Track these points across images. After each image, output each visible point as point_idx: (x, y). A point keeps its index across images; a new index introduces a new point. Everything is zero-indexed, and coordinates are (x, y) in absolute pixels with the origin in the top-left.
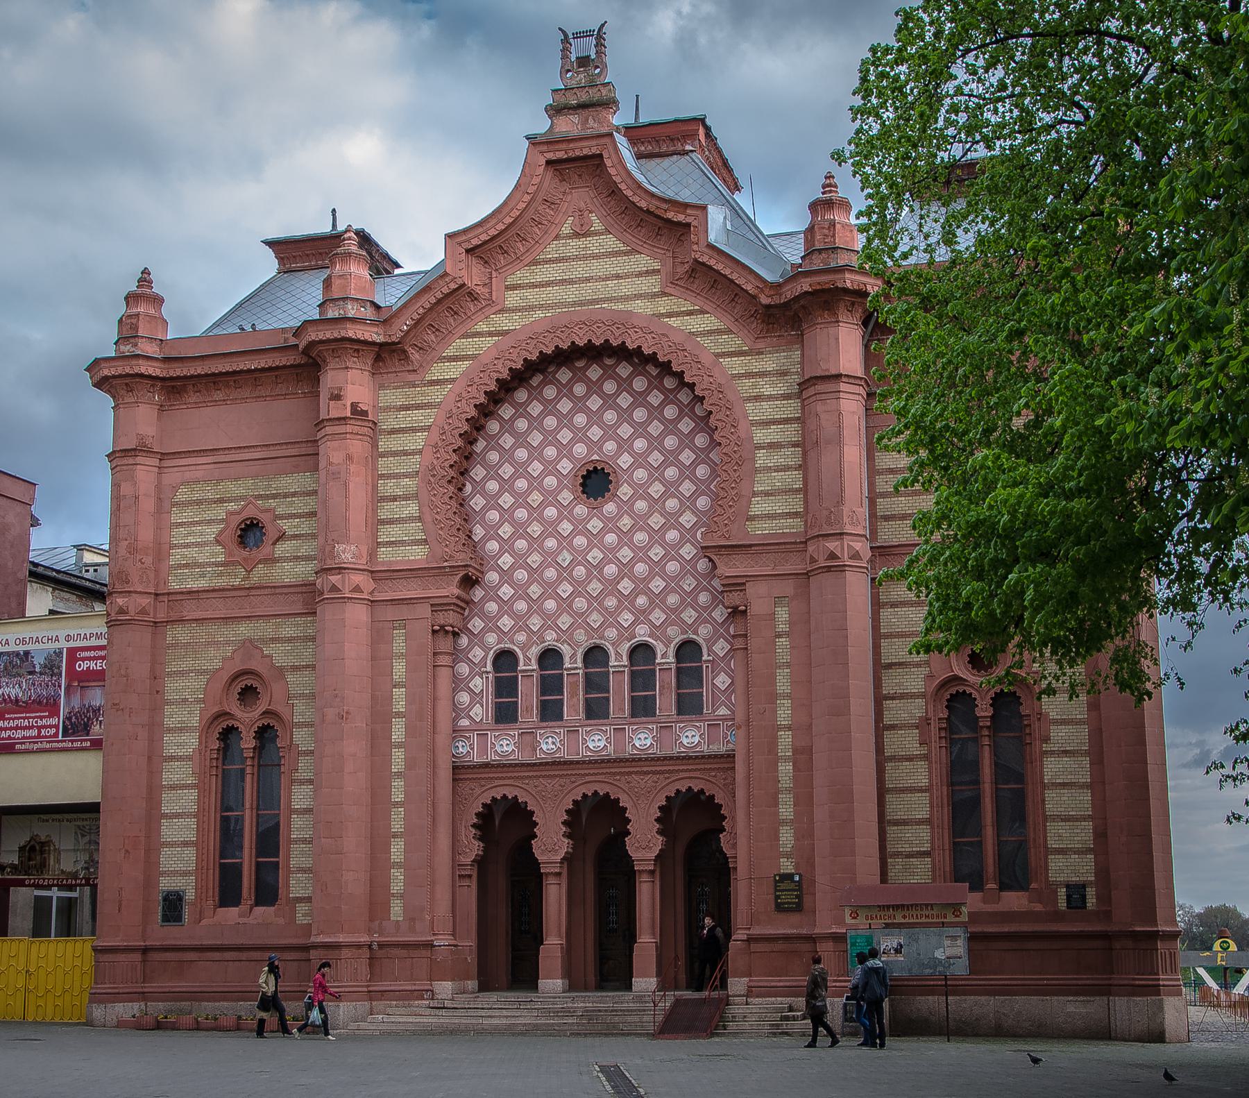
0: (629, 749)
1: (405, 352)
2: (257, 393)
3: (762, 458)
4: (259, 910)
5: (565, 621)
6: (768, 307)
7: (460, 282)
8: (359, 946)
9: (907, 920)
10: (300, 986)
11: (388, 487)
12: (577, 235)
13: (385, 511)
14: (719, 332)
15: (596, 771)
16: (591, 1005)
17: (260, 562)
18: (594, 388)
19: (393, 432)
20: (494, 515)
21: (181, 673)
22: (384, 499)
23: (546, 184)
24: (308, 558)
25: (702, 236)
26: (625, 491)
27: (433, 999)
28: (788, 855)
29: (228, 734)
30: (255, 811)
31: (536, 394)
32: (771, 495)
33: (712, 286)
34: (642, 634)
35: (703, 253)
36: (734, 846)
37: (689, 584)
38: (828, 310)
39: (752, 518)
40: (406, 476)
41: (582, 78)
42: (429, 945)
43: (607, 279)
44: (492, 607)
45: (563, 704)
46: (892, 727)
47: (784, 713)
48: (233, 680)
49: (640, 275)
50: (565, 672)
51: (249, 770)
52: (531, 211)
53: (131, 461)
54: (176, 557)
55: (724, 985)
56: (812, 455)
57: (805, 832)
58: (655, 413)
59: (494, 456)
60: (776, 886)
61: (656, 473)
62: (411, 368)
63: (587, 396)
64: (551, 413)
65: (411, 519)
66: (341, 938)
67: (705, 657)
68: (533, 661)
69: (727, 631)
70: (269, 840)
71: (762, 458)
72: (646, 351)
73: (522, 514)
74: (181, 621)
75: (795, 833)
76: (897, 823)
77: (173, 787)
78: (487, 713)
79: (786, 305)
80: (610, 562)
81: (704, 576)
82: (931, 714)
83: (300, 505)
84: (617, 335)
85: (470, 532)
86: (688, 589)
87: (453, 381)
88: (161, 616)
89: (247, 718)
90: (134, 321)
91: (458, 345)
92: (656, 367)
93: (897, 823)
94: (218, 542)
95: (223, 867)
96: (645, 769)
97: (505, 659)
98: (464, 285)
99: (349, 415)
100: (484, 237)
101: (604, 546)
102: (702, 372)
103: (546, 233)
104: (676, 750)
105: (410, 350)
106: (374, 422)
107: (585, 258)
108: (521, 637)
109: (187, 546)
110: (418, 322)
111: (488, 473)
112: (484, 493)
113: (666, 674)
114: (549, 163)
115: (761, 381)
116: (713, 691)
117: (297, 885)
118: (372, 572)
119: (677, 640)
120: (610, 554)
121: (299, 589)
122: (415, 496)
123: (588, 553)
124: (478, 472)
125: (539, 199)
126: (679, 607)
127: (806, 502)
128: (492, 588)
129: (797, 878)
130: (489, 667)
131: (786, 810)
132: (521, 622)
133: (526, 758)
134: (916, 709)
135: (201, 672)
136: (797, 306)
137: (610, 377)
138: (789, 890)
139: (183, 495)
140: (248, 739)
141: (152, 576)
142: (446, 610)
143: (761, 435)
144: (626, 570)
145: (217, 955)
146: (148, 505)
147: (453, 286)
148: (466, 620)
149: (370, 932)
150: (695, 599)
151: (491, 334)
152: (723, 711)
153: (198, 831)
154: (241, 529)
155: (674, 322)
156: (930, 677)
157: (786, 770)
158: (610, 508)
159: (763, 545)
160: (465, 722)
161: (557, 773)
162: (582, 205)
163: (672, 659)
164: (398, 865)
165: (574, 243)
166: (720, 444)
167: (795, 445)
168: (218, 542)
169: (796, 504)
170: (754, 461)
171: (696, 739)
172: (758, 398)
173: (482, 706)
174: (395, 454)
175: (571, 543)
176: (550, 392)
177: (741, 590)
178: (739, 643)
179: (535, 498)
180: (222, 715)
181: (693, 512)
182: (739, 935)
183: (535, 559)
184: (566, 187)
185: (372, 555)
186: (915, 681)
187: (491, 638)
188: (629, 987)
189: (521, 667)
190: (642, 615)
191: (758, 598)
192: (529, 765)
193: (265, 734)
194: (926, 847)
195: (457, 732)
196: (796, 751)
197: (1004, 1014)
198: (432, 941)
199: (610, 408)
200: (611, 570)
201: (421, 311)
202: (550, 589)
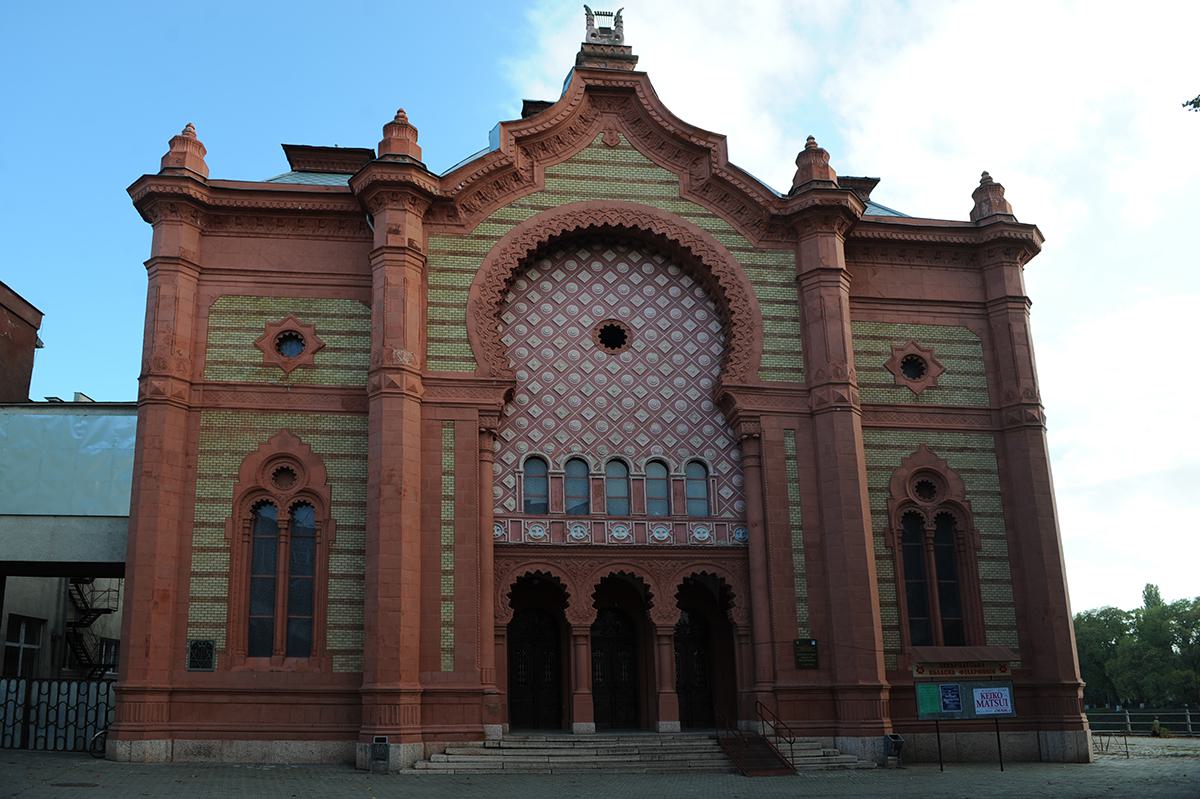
0: (649, 541)
2: (299, 232)
3: (768, 327)
4: (291, 660)
6: (774, 217)
7: (510, 160)
13: (435, 331)
14: (729, 232)
17: (299, 366)
18: (609, 266)
24: (348, 368)
25: (721, 158)
26: (638, 345)
28: (803, 625)
31: (559, 264)
34: (657, 451)
35: (722, 171)
37: (695, 418)
39: (761, 369)
44: (524, 421)
47: (795, 517)
49: (661, 183)
50: (591, 477)
51: (283, 539)
52: (571, 121)
53: (172, 267)
54: (213, 354)
58: (662, 290)
61: (664, 333)
64: (572, 281)
68: (562, 466)
69: (728, 455)
70: (305, 599)
74: (217, 408)
77: (203, 550)
78: (520, 504)
83: (339, 325)
86: (693, 420)
88: (196, 402)
90: (181, 157)
91: (503, 212)
92: (663, 257)
98: (511, 164)
100: (533, 131)
107: (614, 164)
108: (551, 447)
110: (471, 186)
111: (517, 319)
112: (514, 333)
114: (588, 88)
117: (335, 640)
121: (339, 392)
124: (509, 317)
126: (687, 435)
127: (807, 361)
128: (522, 407)
129: (814, 643)
130: (521, 469)
131: (801, 590)
133: (557, 542)
135: (235, 453)
137: (623, 261)
141: (188, 367)
143: (766, 310)
144: (642, 404)
146: (187, 307)
147: (504, 162)
150: (700, 430)
151: (533, 207)
155: (693, 220)
157: (799, 559)
158: (626, 355)
159: (775, 389)
160: (499, 511)
162: (611, 126)
163: (683, 473)
165: (606, 151)
167: (795, 320)
168: (256, 346)
172: (763, 283)
176: (572, 265)
177: (756, 422)
183: (561, 388)
184: (597, 111)
187: (523, 446)
190: (656, 438)
191: (770, 428)
196: (807, 545)
200: (628, 402)
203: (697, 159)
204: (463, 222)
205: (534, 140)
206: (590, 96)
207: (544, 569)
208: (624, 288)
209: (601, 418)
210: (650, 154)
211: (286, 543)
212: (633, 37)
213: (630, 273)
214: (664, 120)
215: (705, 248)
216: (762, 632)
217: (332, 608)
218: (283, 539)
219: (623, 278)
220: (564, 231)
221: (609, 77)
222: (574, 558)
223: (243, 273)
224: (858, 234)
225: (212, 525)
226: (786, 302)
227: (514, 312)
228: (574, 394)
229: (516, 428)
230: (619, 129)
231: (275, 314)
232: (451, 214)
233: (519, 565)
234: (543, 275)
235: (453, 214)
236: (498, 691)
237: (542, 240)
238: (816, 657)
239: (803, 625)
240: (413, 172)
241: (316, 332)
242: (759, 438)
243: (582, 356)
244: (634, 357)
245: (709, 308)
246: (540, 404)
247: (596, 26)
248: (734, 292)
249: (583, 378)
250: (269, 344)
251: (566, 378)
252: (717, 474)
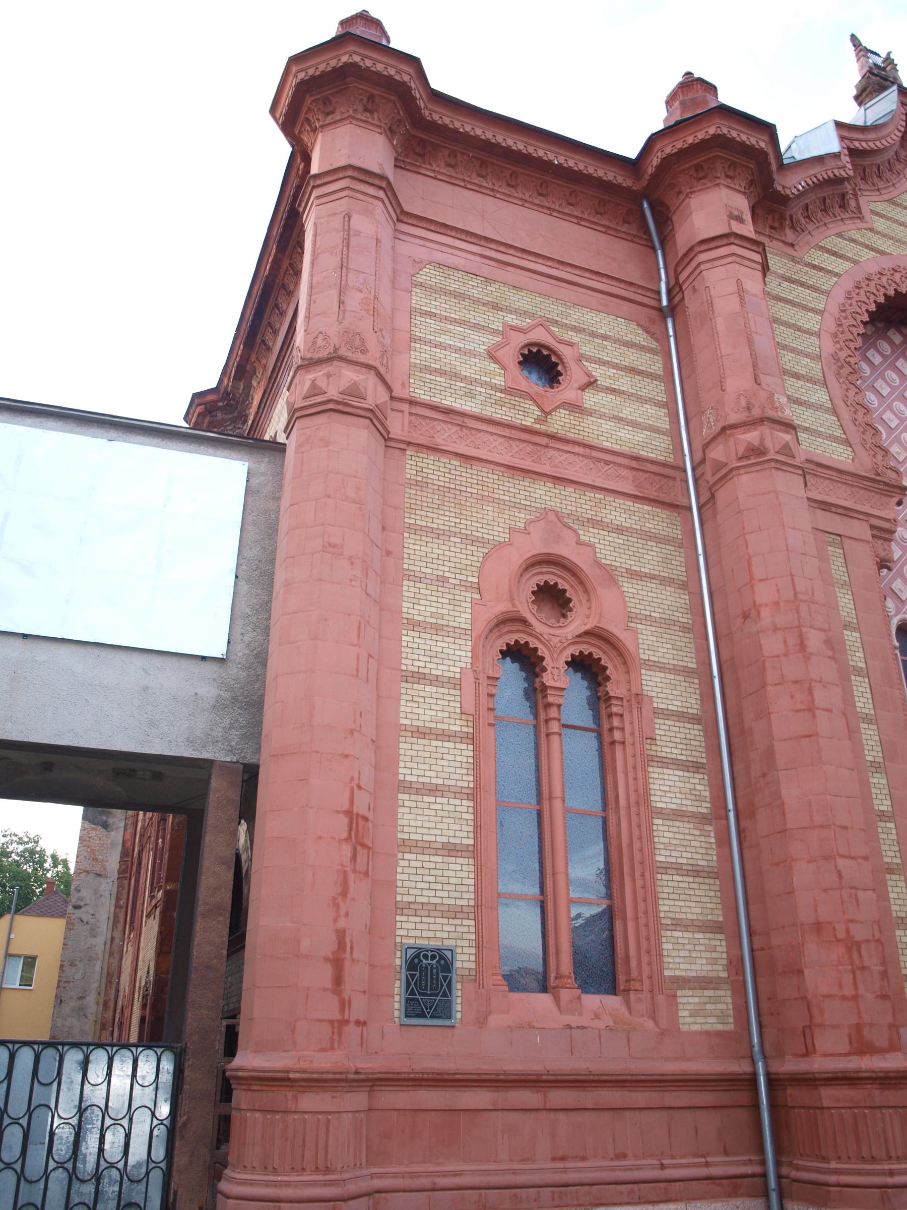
1: (782, 218)
10: (707, 1165)
21: (437, 534)
24: (634, 424)
48: (526, 569)
121: (626, 462)
180: (515, 620)
225: (435, 681)
231: (515, 311)
232: (776, 225)
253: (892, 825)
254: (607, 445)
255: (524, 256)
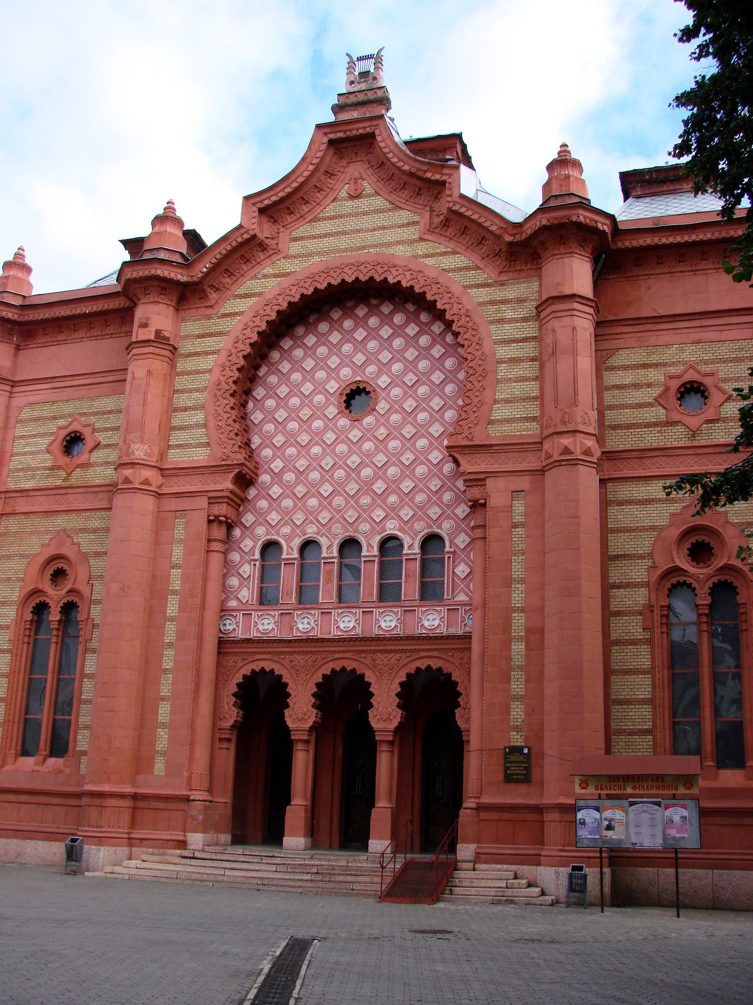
0: (376, 631)
1: (204, 291)
2: (91, 334)
3: (503, 371)
4: (52, 761)
5: (324, 516)
6: (511, 244)
7: (252, 233)
8: (122, 796)
9: (637, 791)
11: (181, 400)
12: (352, 197)
14: (467, 268)
15: (344, 649)
16: (327, 863)
18: (361, 322)
19: (190, 355)
20: (270, 427)
22: (177, 410)
23: (328, 159)
26: (382, 406)
27: (185, 849)
28: (517, 729)
29: (41, 609)
30: (56, 675)
31: (311, 328)
32: (511, 402)
33: (463, 233)
35: (455, 203)
36: (468, 720)
38: (564, 244)
39: (491, 422)
40: (197, 390)
41: (363, 86)
42: (187, 800)
43: (374, 230)
45: (319, 590)
46: (618, 614)
47: (518, 596)
50: (323, 561)
52: (315, 179)
55: (453, 850)
56: (549, 366)
57: (535, 708)
59: (273, 379)
60: (505, 758)
62: (208, 304)
63: (354, 330)
65: (198, 426)
66: (106, 788)
67: (447, 549)
68: (295, 551)
71: (503, 371)
72: (405, 284)
73: (293, 426)
75: (525, 708)
76: (620, 702)
79: (525, 244)
80: (367, 466)
81: (448, 478)
82: (653, 601)
83: (113, 421)
84: (380, 272)
85: (249, 440)
87: (242, 313)
89: (55, 596)
91: (249, 285)
92: (413, 304)
93: (620, 702)
94: (48, 451)
95: (26, 720)
96: (389, 648)
97: (270, 547)
99: (152, 337)
100: (274, 199)
101: (362, 453)
102: (452, 301)
103: (326, 196)
104: (419, 631)
105: (209, 290)
106: (173, 346)
107: (357, 215)
108: (286, 530)
109: (25, 454)
113: (410, 564)
114: (331, 142)
115: (503, 307)
116: (453, 579)
117: (82, 741)
118: (161, 470)
119: (422, 534)
120: (367, 459)
122: (202, 407)
123: (347, 459)
124: (259, 392)
125: (322, 170)
127: (542, 407)
129: (526, 751)
130: (257, 556)
131: (518, 686)
132: (287, 516)
133: (286, 636)
134: (639, 597)
135: (23, 556)
136: (536, 243)
137: (375, 314)
138: (517, 762)
139: (26, 414)
140: (55, 613)
142: (221, 503)
143: (503, 352)
145: (12, 797)
147: (246, 236)
148: (239, 515)
149: (133, 784)
150: (440, 499)
151: (275, 276)
152: (462, 597)
153: (8, 689)
154: (67, 441)
155: (429, 261)
156: (654, 567)
157: (518, 649)
158: (369, 420)
160: (233, 604)
161: (310, 649)
162: (356, 175)
163: (417, 550)
164: (163, 725)
166: (466, 359)
167: (533, 360)
168: (48, 451)
169: (533, 410)
170: (496, 372)
171: (436, 623)
172: (501, 321)
173: (249, 589)
174: (189, 373)
175: (333, 451)
176: (323, 327)
177: (481, 485)
178: (479, 533)
179: (306, 413)
181: (441, 424)
182: (469, 803)
183: (302, 464)
184: (344, 162)
185: (162, 456)
186: (639, 572)
187: (260, 531)
188: (365, 848)
189: (284, 556)
190: (392, 512)
192: (285, 641)
193: (69, 608)
194: (648, 725)
195: (224, 612)
196: (529, 631)
197: (722, 888)
198: (189, 796)
199: (373, 338)
200: (366, 472)
201: (219, 256)
202: (313, 490)
203: (438, 193)
204: (213, 302)
205: (280, 207)
206: (336, 149)
207: (268, 666)
208: (372, 345)
209: (339, 494)
210: (393, 197)
211: (57, 643)
212: (388, 79)
213: (380, 327)
214: (400, 160)
215: (442, 290)
216: (474, 740)
217: (85, 709)
218: (54, 639)
219: (372, 334)
220: (302, 295)
221: (350, 127)
222: (299, 653)
223: (44, 382)
224: (620, 245)
226: (525, 340)
227: (265, 385)
228: (314, 469)
229: (256, 510)
230: (364, 176)
232: (203, 296)
233: (246, 661)
234: (295, 342)
235: (203, 296)
236: (210, 798)
237: (281, 308)
238: (528, 769)
239: (517, 729)
240: (157, 266)
241: (94, 431)
242: (484, 505)
243: (326, 425)
244: (377, 420)
245: (459, 354)
246: (280, 483)
247: (357, 73)
248: (467, 336)
249: (324, 450)
250: (57, 448)
251: (308, 453)
252: (452, 550)
253: (171, 676)
254: (98, 482)
255: (73, 378)
